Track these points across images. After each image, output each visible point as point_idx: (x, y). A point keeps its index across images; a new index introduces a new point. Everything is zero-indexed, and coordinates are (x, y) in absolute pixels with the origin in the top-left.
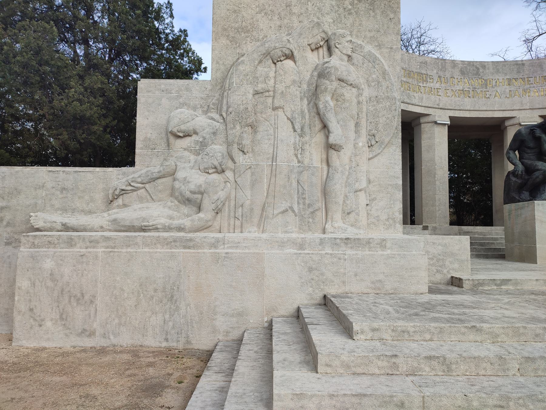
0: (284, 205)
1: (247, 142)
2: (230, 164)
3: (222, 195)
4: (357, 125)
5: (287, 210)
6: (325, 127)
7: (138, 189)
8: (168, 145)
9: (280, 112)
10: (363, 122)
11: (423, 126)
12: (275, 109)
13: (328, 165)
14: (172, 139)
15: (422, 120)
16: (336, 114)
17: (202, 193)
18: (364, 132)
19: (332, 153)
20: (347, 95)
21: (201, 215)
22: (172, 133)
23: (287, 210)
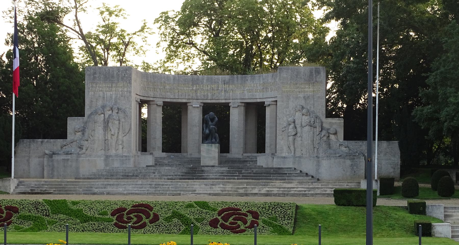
0: (101, 149)
1: (93, 134)
2: (89, 139)
3: (87, 146)
4: (119, 129)
5: (102, 150)
6: (111, 130)
7: (68, 145)
8: (75, 134)
9: (100, 127)
10: (121, 128)
11: (189, 107)
12: (99, 126)
13: (112, 138)
14: (76, 132)
15: (188, 104)
16: (113, 127)
17: (83, 146)
18: (121, 130)
19: (113, 136)
20: (116, 123)
21: (83, 151)
22: (76, 131)
23: (102, 150)
